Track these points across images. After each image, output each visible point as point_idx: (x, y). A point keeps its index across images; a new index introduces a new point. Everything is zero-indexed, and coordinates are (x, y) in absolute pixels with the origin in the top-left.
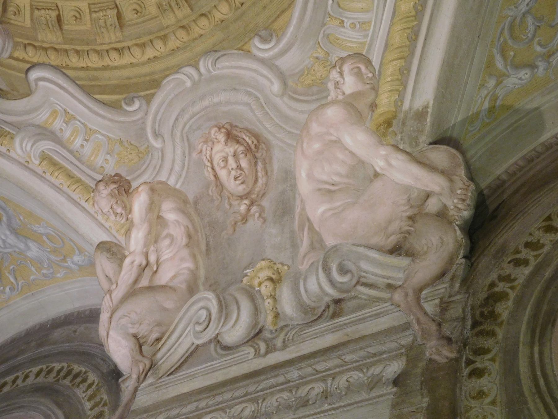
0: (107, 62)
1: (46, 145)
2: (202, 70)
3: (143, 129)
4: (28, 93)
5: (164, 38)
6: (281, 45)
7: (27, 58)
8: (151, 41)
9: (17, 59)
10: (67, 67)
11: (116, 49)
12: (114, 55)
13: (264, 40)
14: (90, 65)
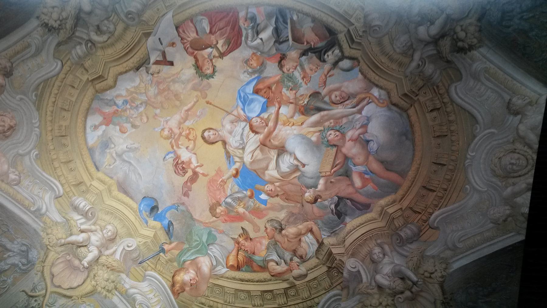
0: (53, 95)
1: (33, 49)
2: (36, 129)
3: (25, 95)
4: (54, 57)
5: (51, 121)
6: (32, 160)
7: (66, 65)
8: (52, 116)
9: (67, 61)
10: (57, 79)
11: (55, 102)
12: (54, 100)
13: (36, 155)
14: (54, 88)
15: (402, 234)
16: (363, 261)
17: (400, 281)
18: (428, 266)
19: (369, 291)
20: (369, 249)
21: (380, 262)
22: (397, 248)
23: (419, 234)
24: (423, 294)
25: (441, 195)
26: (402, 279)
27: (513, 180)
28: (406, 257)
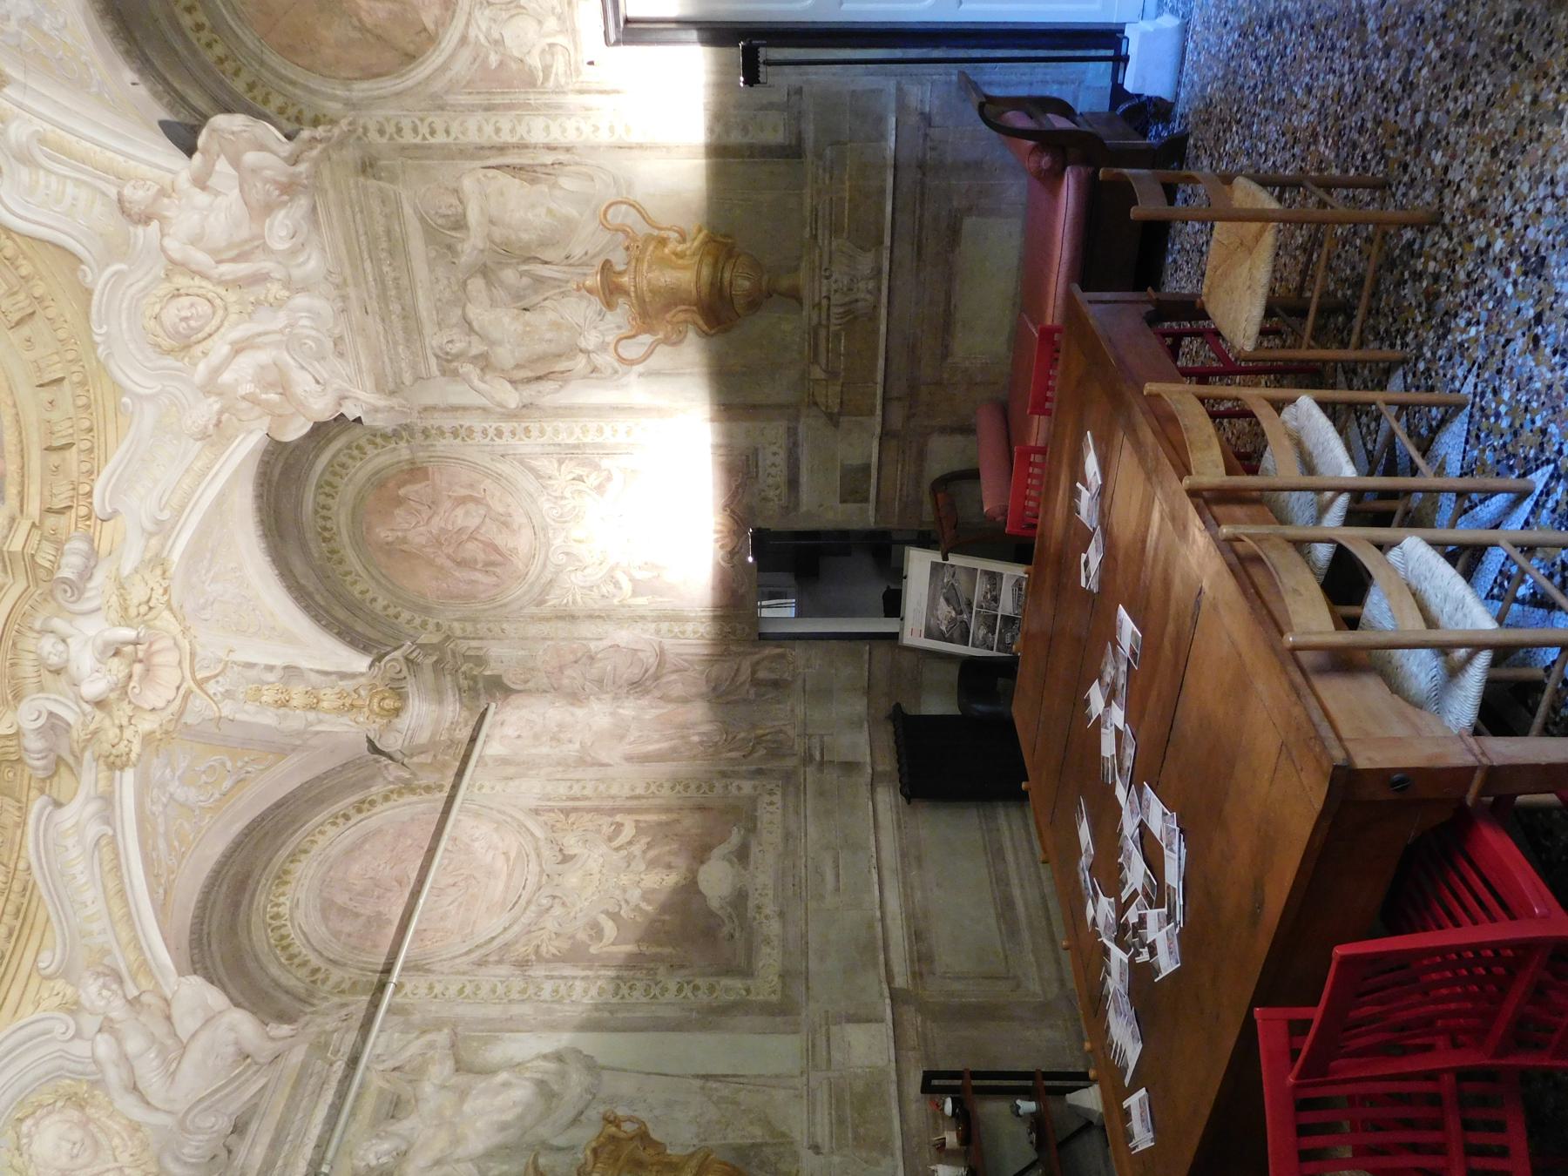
15: (65, 573)
16: (42, 689)
17: (115, 663)
18: (137, 594)
19: (92, 727)
20: (32, 656)
21: (68, 661)
22: (77, 607)
23: (92, 548)
24: (155, 647)
25: (88, 444)
26: (116, 653)
27: (200, 348)
28: (99, 609)
